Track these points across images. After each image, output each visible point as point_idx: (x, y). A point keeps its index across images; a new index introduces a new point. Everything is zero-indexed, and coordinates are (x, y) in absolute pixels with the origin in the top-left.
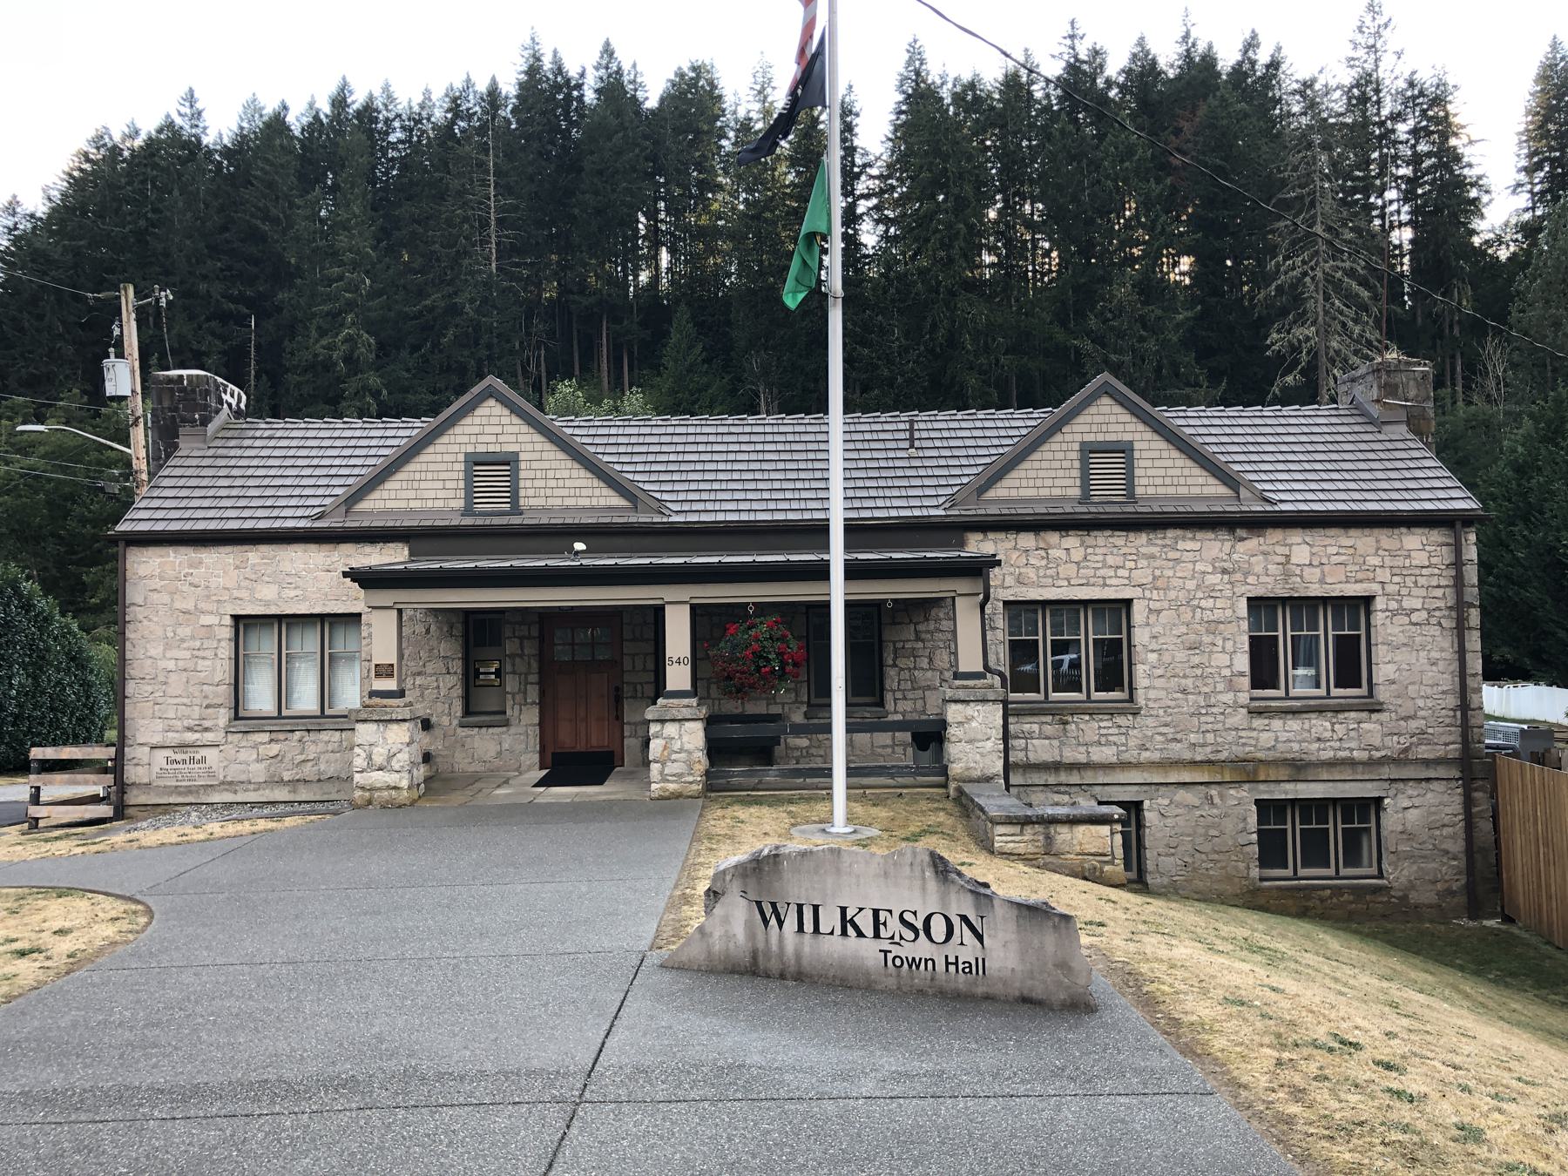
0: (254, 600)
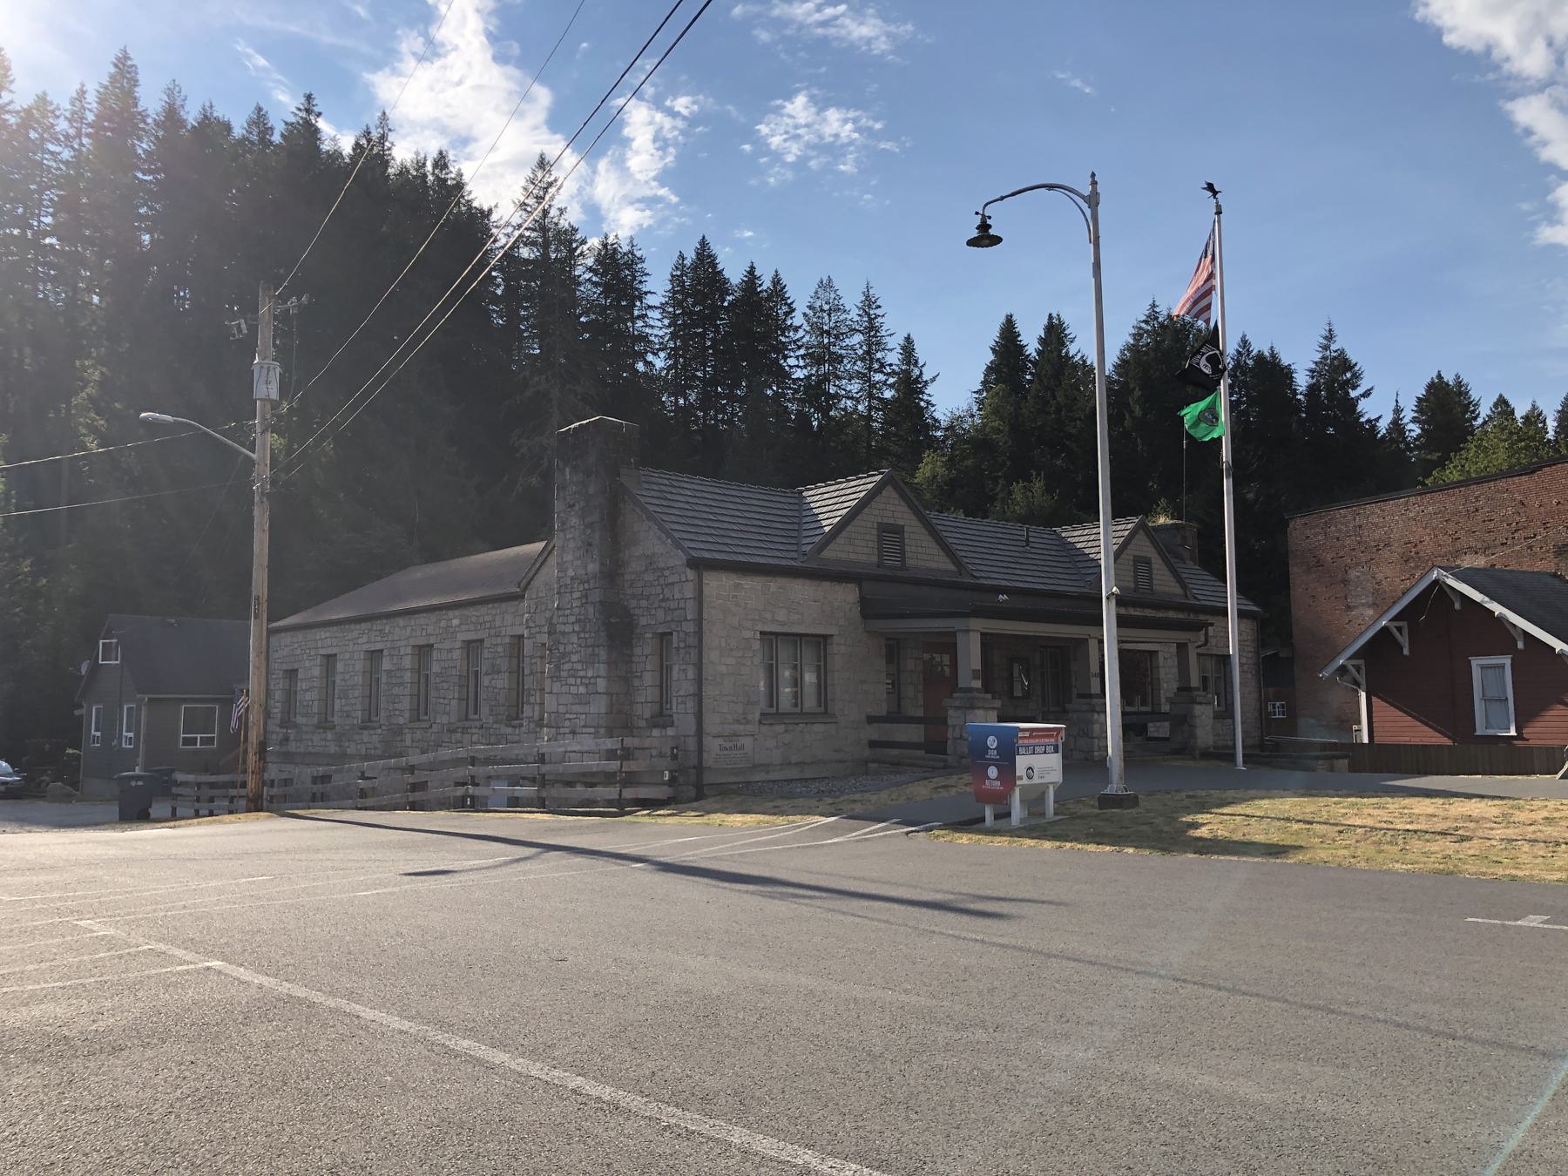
0: (773, 621)
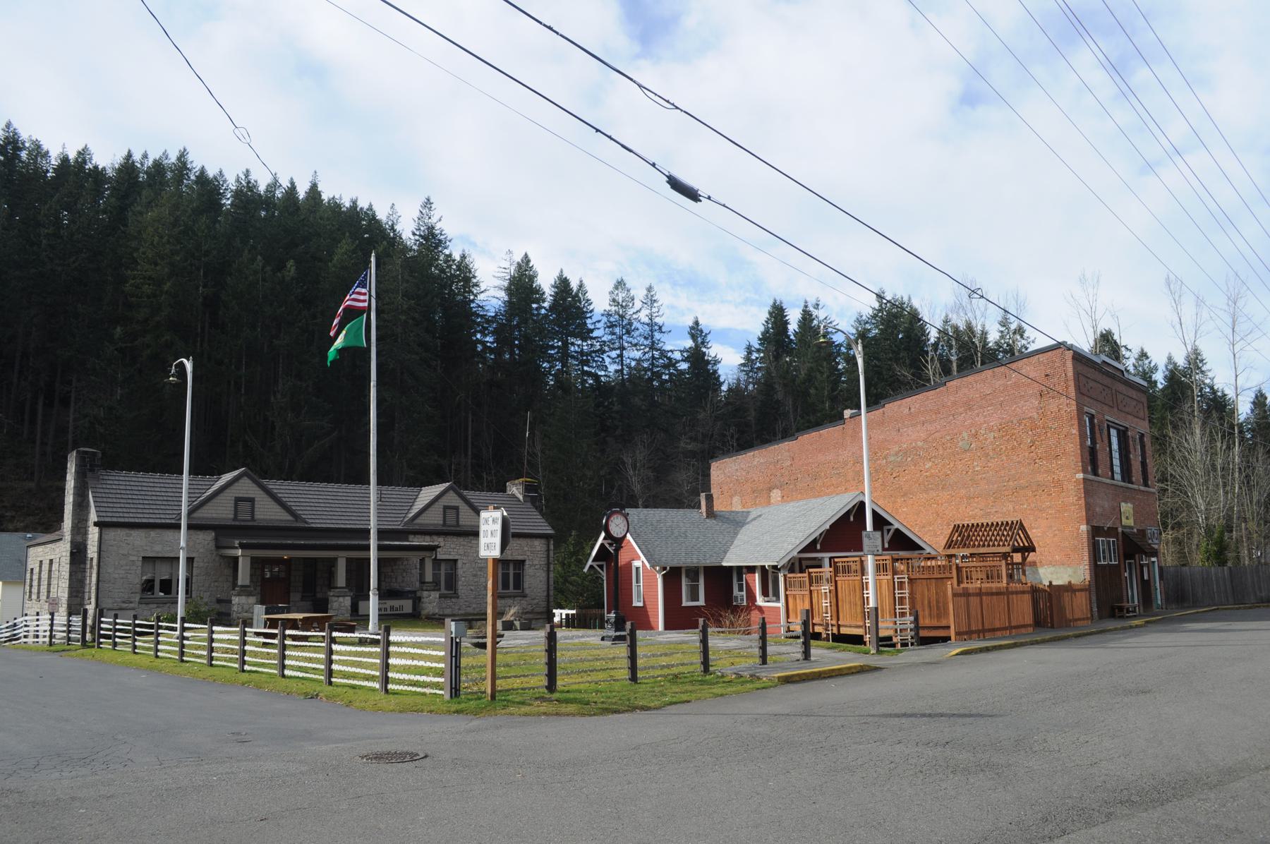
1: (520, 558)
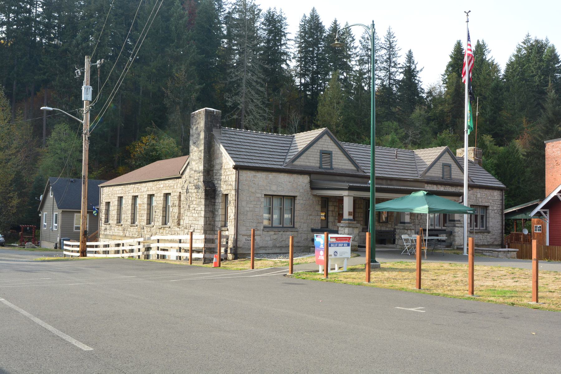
0: (270, 190)
1: (486, 204)
